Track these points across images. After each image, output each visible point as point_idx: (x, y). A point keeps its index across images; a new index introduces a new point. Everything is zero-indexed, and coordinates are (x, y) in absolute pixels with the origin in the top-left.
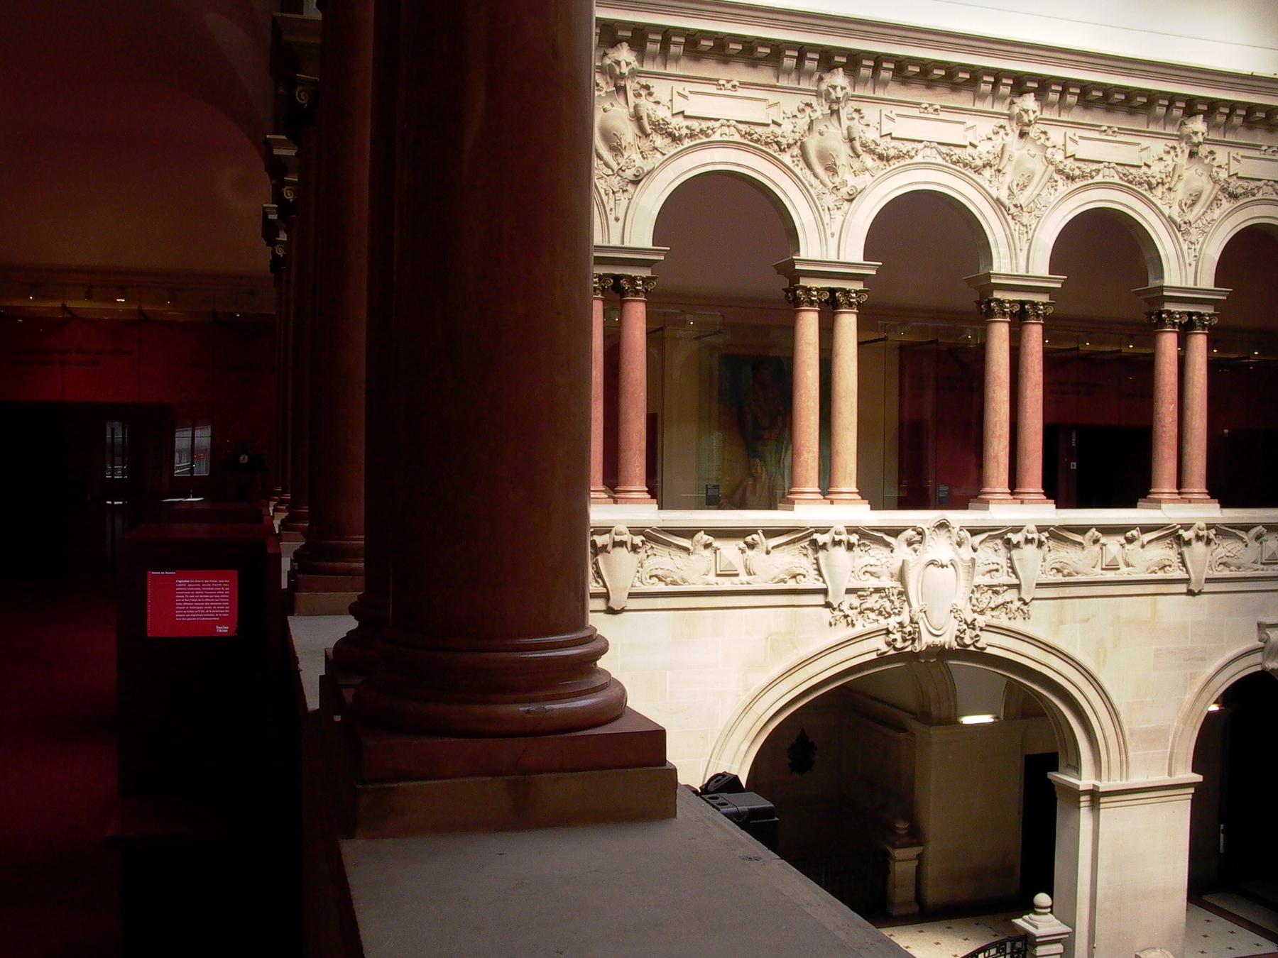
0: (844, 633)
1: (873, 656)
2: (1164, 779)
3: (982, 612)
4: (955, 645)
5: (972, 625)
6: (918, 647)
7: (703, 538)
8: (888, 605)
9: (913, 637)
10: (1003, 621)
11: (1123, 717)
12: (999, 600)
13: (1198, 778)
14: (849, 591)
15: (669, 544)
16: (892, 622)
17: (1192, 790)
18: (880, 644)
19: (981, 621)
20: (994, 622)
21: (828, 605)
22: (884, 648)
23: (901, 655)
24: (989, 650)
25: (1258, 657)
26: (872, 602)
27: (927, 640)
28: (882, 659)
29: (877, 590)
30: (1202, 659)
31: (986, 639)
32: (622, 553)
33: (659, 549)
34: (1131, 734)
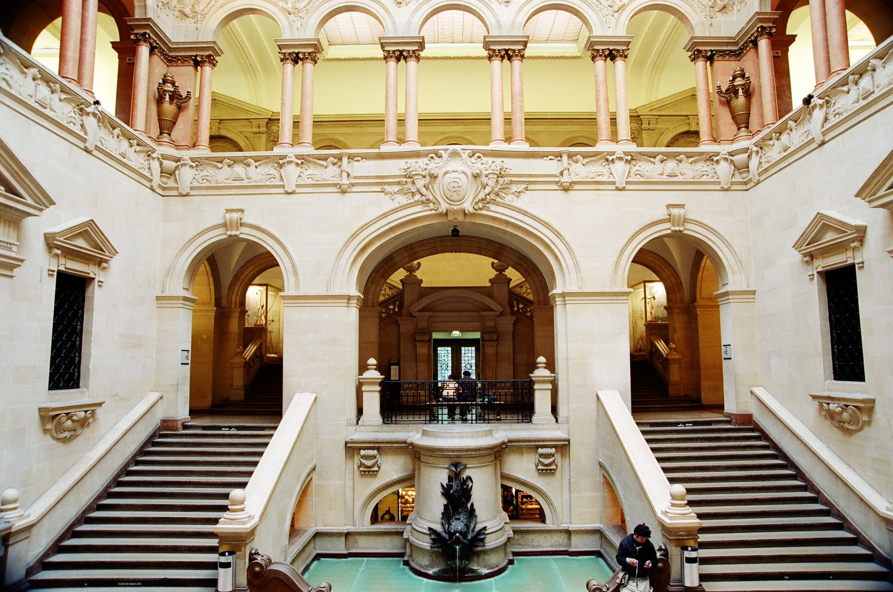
7: (331, 159)
15: (315, 163)
25: (668, 225)
32: (293, 166)
33: (312, 166)
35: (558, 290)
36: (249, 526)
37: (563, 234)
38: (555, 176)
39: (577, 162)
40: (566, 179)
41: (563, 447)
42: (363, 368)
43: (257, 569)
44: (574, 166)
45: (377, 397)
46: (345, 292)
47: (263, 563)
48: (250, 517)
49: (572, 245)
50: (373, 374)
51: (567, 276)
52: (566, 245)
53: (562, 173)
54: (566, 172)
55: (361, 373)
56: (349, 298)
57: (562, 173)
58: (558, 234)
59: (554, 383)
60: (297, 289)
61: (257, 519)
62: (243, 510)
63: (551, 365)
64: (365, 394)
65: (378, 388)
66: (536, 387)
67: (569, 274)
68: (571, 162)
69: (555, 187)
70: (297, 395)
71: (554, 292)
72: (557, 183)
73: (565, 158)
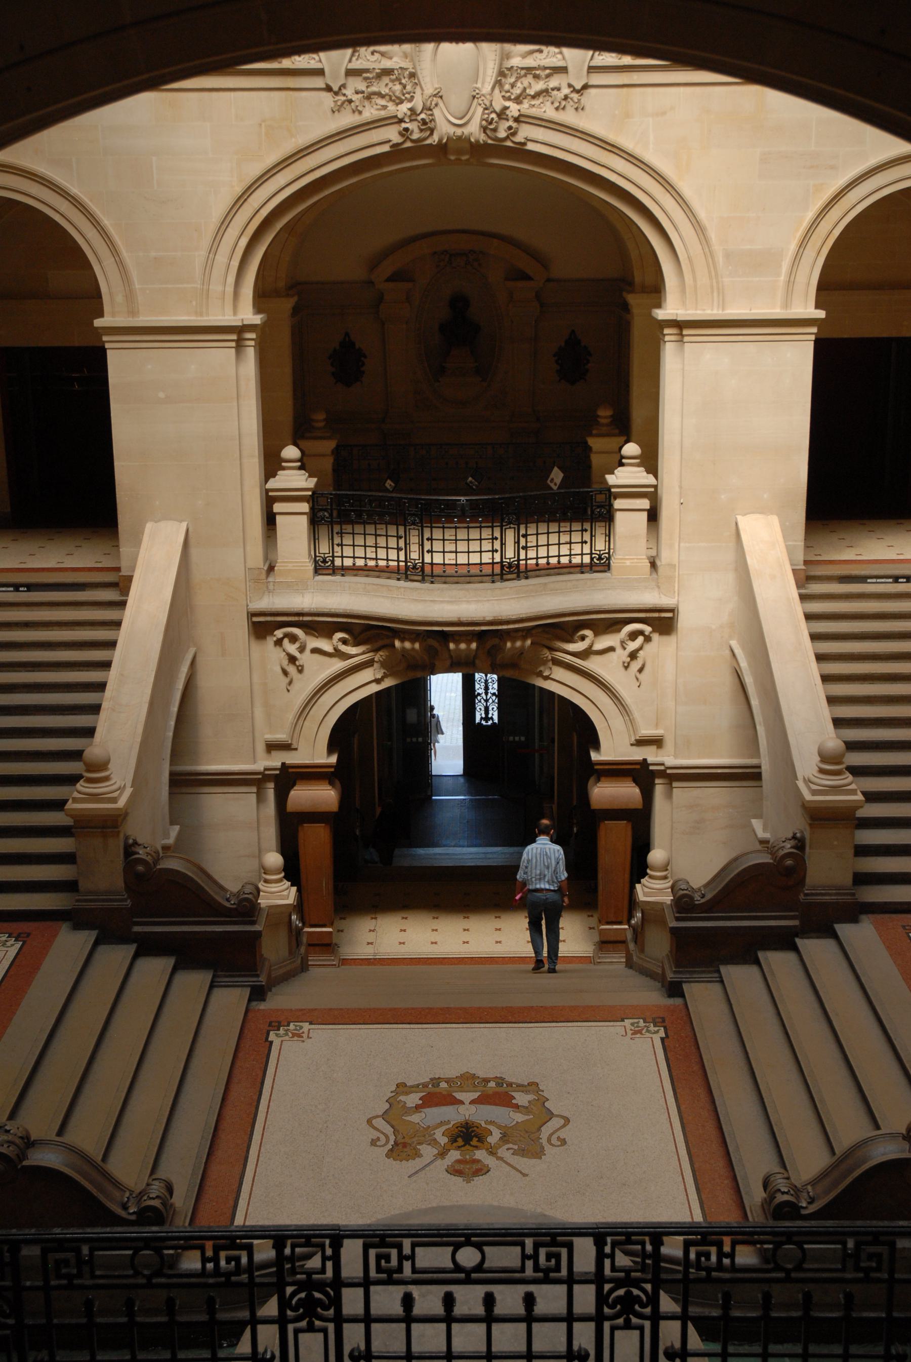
0: (347, 119)
1: (386, 148)
2: (777, 312)
3: (518, 100)
4: (482, 138)
5: (502, 114)
6: (435, 139)
8: (398, 88)
9: (428, 126)
10: (547, 110)
11: (712, 234)
12: (539, 86)
13: (821, 314)
14: (350, 73)
16: (404, 108)
17: (814, 330)
18: (392, 134)
19: (514, 109)
20: (534, 112)
21: (329, 89)
22: (396, 139)
23: (420, 150)
24: (531, 146)
26: (381, 87)
27: (444, 129)
28: (397, 153)
29: (387, 72)
30: (833, 167)
31: (525, 132)
34: (728, 255)
35: (672, 308)
36: (121, 803)
41: (663, 622)
42: (272, 464)
43: (140, 868)
45: (304, 521)
46: (227, 318)
47: (149, 859)
48: (122, 789)
50: (294, 479)
55: (266, 482)
56: (240, 330)
59: (654, 496)
60: (133, 313)
61: (129, 791)
62: (107, 779)
63: (650, 461)
64: (279, 519)
65: (305, 507)
66: (618, 504)
70: (149, 526)
71: (661, 314)
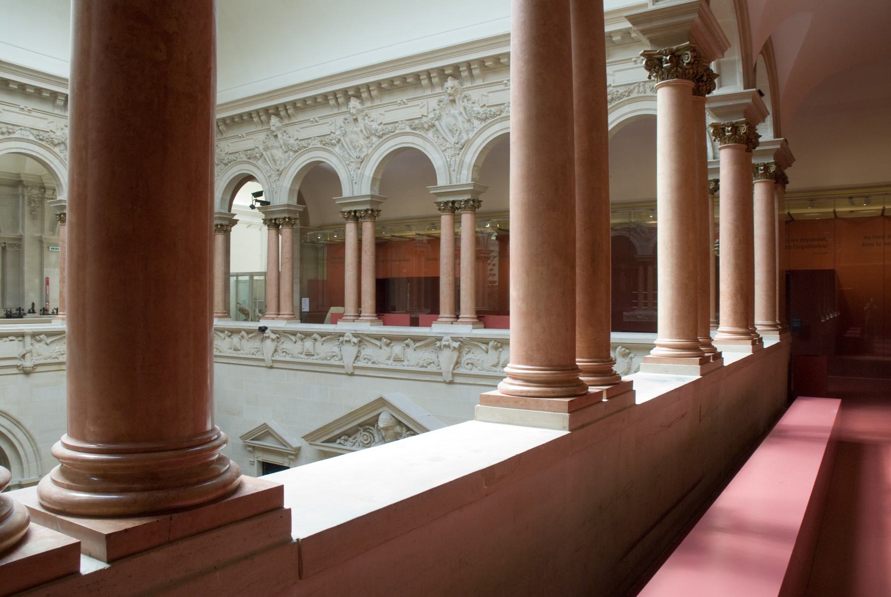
37: (23, 422)
38: (15, 358)
39: (40, 341)
40: (28, 363)
44: (37, 345)
49: (32, 432)
51: (25, 466)
52: (27, 433)
53: (23, 356)
54: (28, 356)
57: (23, 356)
58: (17, 423)
67: (28, 463)
68: (34, 342)
69: (15, 371)
72: (17, 367)
73: (28, 339)
